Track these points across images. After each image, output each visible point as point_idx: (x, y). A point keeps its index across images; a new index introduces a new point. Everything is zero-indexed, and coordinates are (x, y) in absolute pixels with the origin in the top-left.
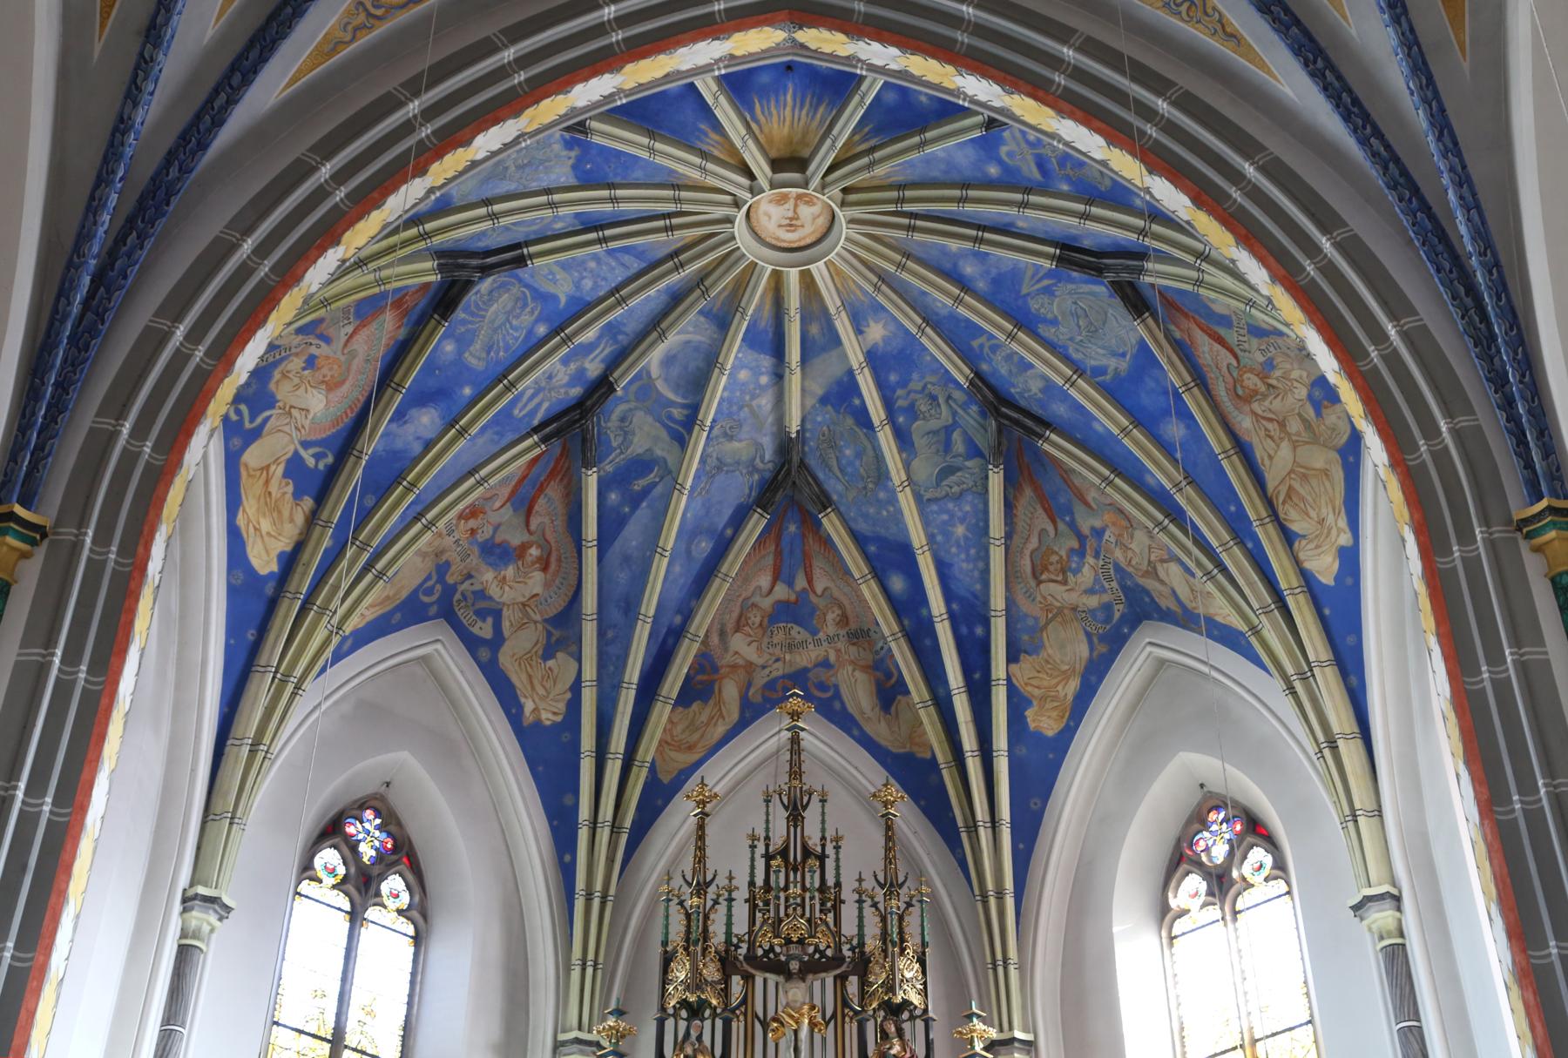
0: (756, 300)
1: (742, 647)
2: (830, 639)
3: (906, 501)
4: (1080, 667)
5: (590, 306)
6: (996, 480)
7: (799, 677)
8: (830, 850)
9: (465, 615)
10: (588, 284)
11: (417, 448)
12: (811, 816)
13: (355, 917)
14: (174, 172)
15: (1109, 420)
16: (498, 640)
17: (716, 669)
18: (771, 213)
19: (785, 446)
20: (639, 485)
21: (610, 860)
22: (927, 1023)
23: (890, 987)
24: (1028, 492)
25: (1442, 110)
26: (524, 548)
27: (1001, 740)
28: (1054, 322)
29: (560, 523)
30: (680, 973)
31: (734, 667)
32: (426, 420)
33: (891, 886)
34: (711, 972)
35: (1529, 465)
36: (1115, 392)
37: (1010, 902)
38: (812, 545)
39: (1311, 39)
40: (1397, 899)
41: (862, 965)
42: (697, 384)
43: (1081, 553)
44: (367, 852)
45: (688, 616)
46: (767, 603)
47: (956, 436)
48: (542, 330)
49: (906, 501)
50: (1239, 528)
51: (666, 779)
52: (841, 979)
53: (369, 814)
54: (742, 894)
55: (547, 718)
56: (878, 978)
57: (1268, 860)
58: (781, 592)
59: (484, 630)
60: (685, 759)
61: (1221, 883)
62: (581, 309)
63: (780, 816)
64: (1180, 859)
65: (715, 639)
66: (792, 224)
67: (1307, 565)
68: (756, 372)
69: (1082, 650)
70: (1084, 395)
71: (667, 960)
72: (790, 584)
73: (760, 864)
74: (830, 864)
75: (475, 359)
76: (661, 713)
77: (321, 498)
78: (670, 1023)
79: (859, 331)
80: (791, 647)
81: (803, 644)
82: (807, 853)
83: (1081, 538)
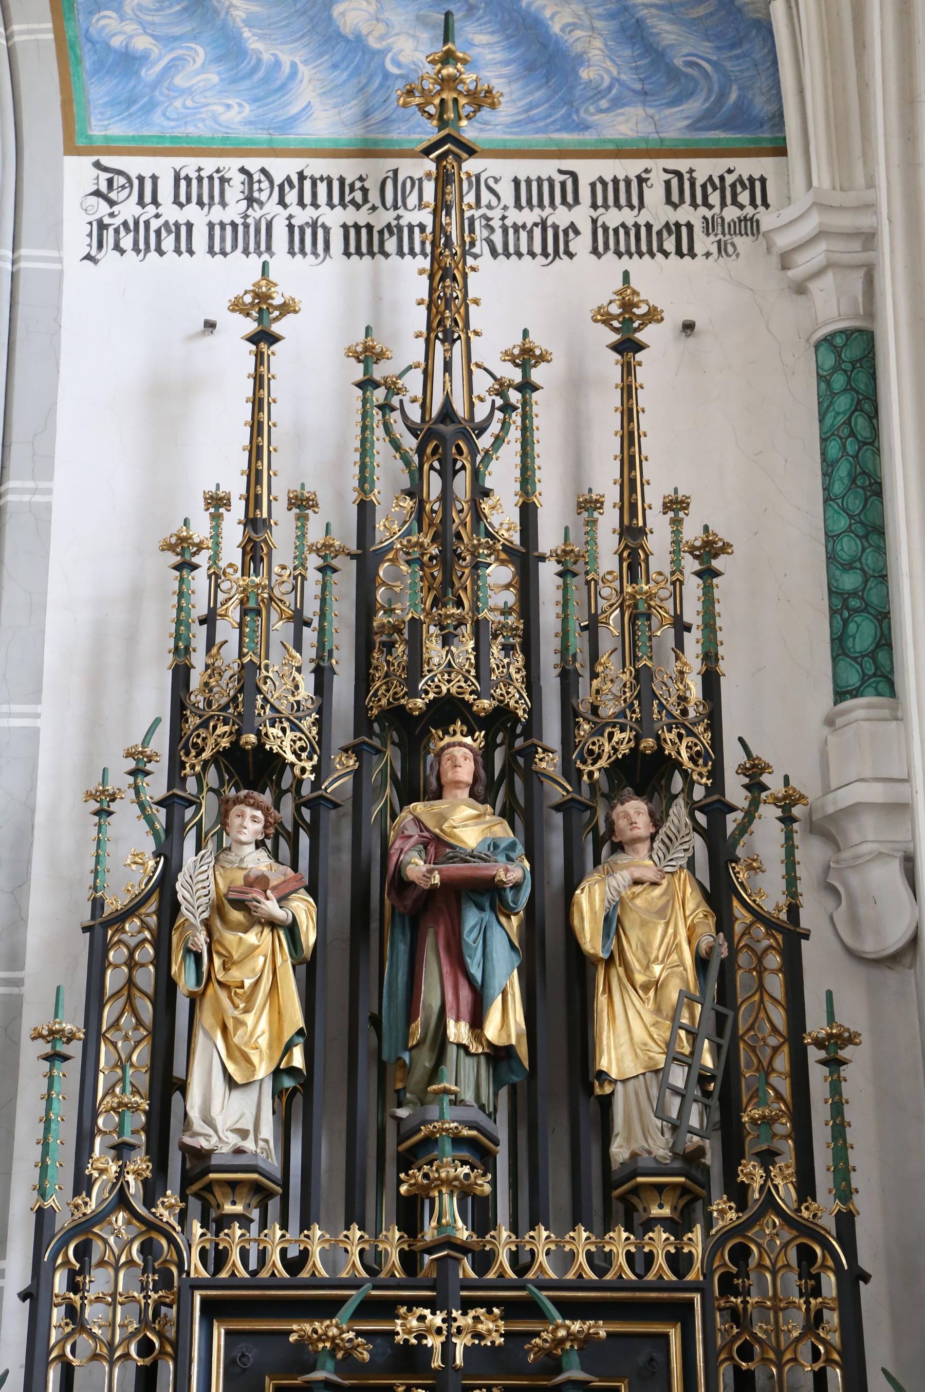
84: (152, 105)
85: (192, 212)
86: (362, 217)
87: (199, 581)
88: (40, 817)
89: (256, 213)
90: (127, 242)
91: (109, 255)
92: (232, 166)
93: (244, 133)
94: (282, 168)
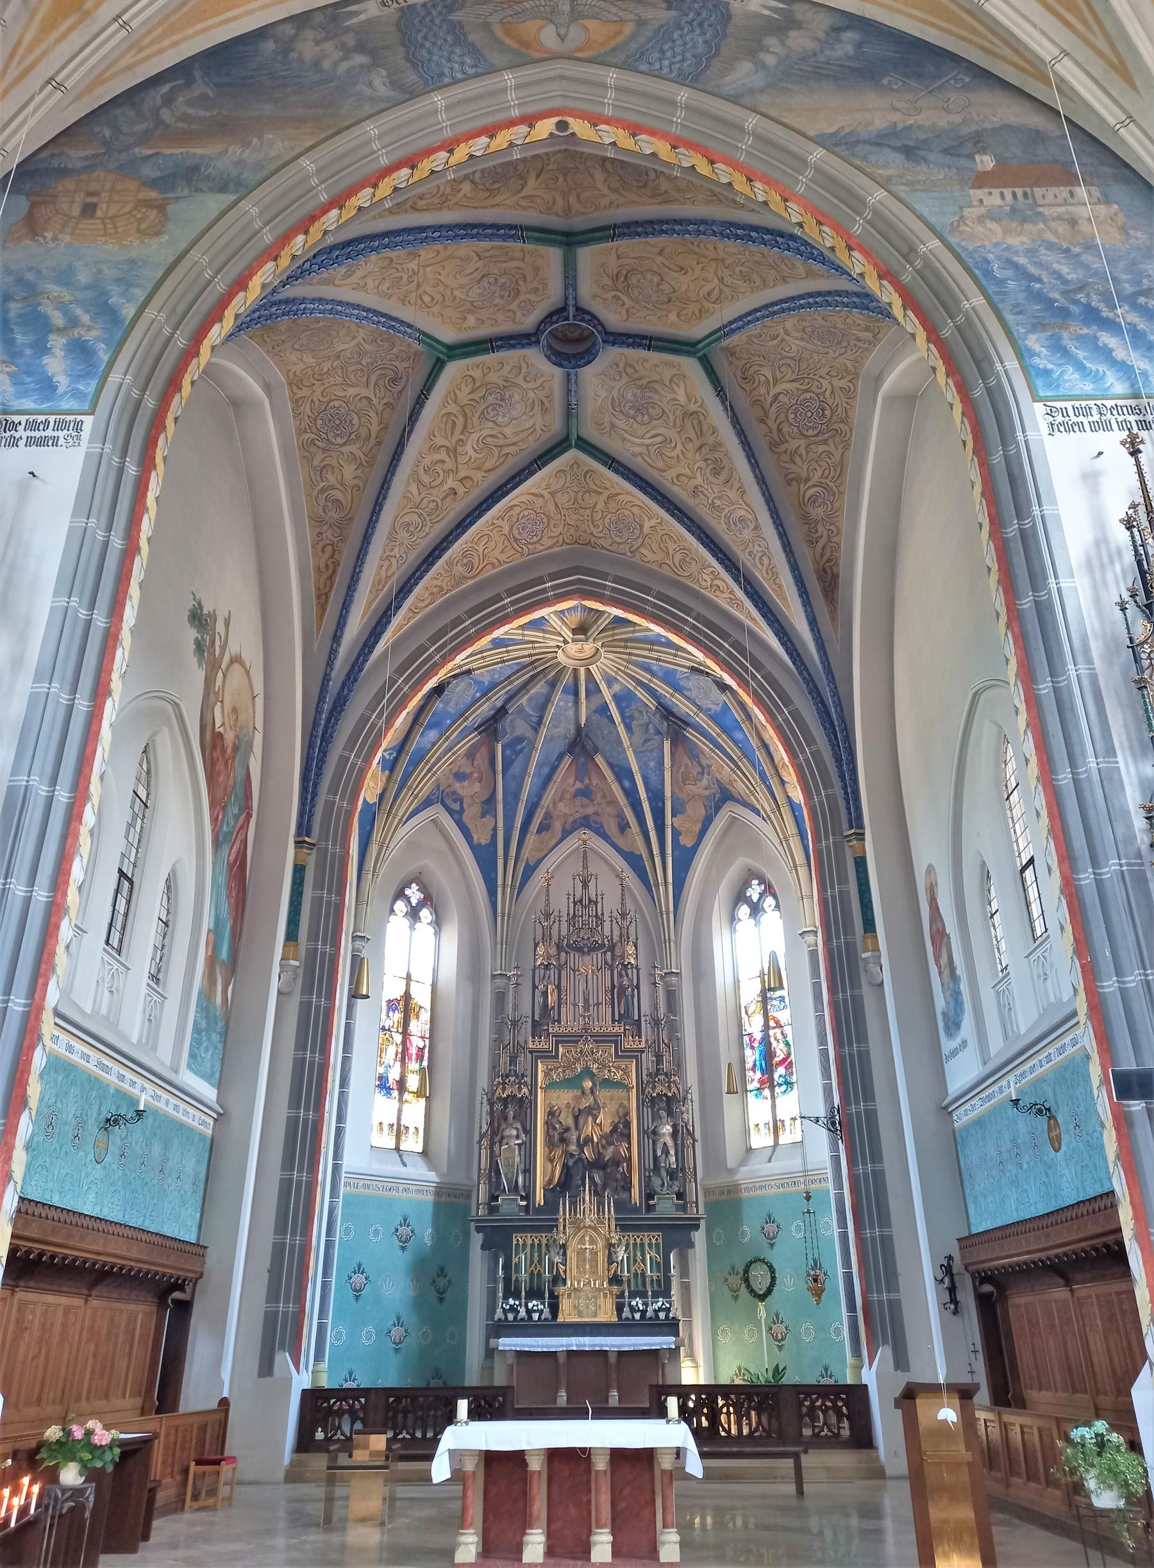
0: (567, 678)
1: (562, 808)
2: (599, 804)
3: (630, 754)
4: (702, 819)
5: (497, 684)
6: (667, 745)
7: (586, 818)
8: (599, 900)
9: (448, 802)
10: (497, 676)
11: (429, 746)
12: (592, 884)
13: (412, 928)
14: (346, 691)
15: (713, 730)
16: (462, 811)
17: (551, 818)
18: (572, 648)
19: (578, 728)
20: (519, 747)
21: (511, 900)
22: (638, 970)
23: (622, 957)
24: (681, 749)
25: (829, 664)
26: (472, 773)
27: (669, 850)
28: (690, 690)
29: (487, 762)
30: (541, 950)
31: (559, 816)
32: (432, 735)
33: (623, 915)
34: (553, 951)
35: (850, 813)
36: (713, 718)
37: (672, 916)
38: (590, 766)
39: (783, 628)
40: (816, 932)
41: (612, 948)
42: (543, 708)
43: (702, 773)
44: (414, 902)
45: (540, 798)
46: (572, 790)
47: (650, 726)
48: (478, 695)
49: (630, 754)
51: (532, 864)
52: (605, 953)
53: (414, 885)
54: (564, 918)
55: (484, 842)
56: (618, 952)
57: (773, 903)
58: (578, 785)
59: (456, 807)
60: (540, 855)
61: (756, 910)
62: (494, 685)
63: (579, 885)
64: (740, 897)
65: (551, 806)
66: (581, 651)
68: (567, 702)
69: (703, 812)
70: (702, 720)
71: (536, 945)
72: (582, 781)
73: (572, 905)
74: (599, 905)
75: (451, 709)
76: (531, 839)
77: (392, 771)
78: (537, 971)
79: (609, 686)
80: (583, 806)
81: (587, 805)
82: (590, 901)
83: (703, 768)
84: (1058, 386)
85: (1081, 419)
86: (1141, 418)
87: (1136, 533)
88: (1085, 616)
89: (1104, 418)
90: (1062, 429)
91: (1057, 433)
92: (1091, 403)
93: (1092, 392)
94: (1109, 403)
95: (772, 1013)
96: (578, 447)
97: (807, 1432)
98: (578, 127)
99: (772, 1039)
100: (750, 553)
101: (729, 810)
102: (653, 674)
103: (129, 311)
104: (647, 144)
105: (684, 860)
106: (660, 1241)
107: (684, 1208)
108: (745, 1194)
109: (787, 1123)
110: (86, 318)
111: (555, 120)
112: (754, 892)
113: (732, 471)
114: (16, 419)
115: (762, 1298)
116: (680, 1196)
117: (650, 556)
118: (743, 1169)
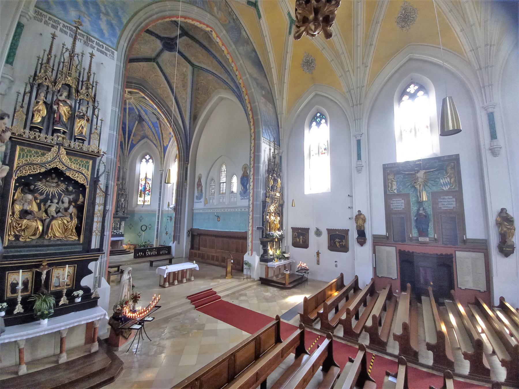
6: (137, 122)
43: (142, 131)
50: (159, 138)
57: (152, 161)
61: (147, 161)
64: (143, 157)
67: (164, 144)
95: (147, 181)
96: (156, 63)
97: (161, 253)
98: (213, 33)
99: (146, 186)
100: (182, 105)
101: (145, 140)
102: (142, 109)
103: (125, 21)
104: (223, 48)
105: (133, 146)
106: (119, 220)
107: (124, 214)
108: (136, 212)
109: (147, 201)
110: (112, 14)
111: (211, 29)
112: (148, 157)
113: (187, 88)
114: (93, 39)
115: (144, 231)
116: (124, 212)
117: (159, 91)
118: (136, 208)
